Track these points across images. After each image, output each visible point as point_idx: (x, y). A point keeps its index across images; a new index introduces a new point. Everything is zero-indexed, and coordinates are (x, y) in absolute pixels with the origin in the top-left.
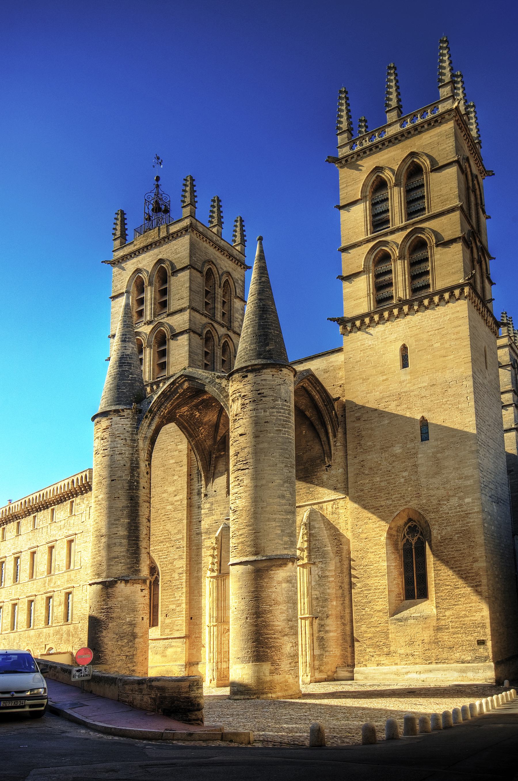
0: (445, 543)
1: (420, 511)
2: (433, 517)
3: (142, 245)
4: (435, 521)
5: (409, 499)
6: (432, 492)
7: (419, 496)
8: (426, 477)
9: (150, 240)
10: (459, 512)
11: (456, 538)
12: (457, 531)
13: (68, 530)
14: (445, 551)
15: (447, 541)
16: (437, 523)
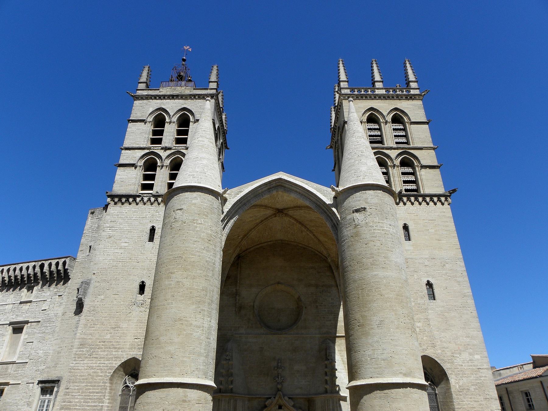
0: (463, 393)
1: (436, 359)
2: (449, 367)
3: (168, 93)
4: (452, 371)
5: (425, 347)
6: (445, 345)
7: (434, 346)
8: (438, 331)
9: (175, 93)
10: (471, 366)
11: (472, 388)
12: (473, 383)
13: (17, 315)
14: (465, 400)
15: (465, 391)
16: (454, 373)
